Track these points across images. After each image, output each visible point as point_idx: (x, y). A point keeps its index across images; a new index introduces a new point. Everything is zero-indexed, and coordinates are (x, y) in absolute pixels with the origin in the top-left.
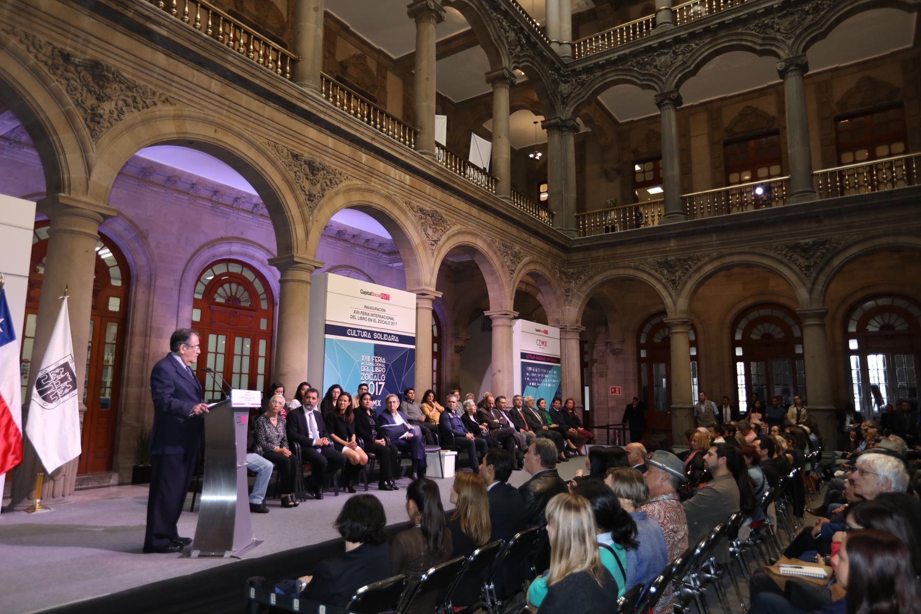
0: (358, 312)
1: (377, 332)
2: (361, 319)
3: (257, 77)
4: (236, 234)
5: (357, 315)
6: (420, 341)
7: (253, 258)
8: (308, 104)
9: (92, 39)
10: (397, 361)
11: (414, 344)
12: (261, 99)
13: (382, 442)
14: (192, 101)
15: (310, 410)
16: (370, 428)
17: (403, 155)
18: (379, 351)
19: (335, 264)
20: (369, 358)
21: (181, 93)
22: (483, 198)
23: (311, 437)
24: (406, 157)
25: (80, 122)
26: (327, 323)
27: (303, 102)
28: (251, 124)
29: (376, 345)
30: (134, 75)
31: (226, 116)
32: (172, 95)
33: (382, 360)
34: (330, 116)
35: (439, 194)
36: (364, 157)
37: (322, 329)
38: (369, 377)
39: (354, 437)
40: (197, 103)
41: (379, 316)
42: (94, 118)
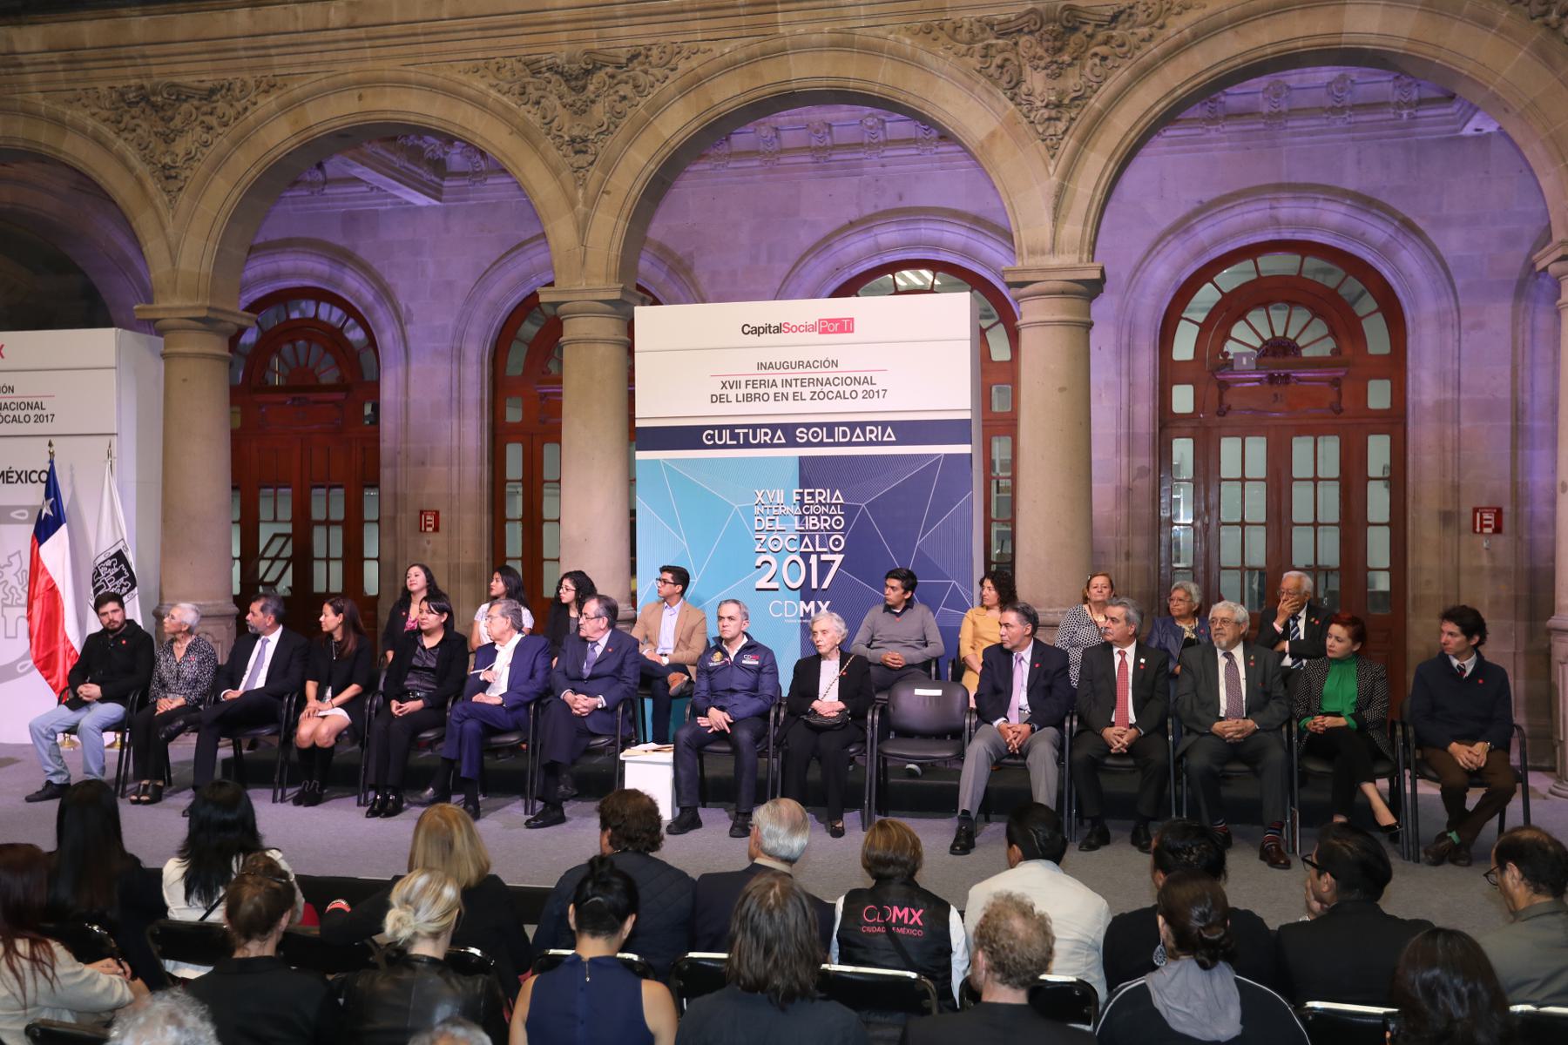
1: (808, 426)
2: (748, 398)
4: (887, 203)
5: (732, 393)
7: (936, 246)
9: (148, 50)
14: (309, 64)
18: (811, 474)
19: (1207, 197)
20: (784, 493)
21: (288, 59)
25: (152, 185)
29: (801, 459)
30: (215, 71)
31: (373, 59)
32: (277, 72)
40: (318, 63)
41: (811, 382)
42: (168, 174)
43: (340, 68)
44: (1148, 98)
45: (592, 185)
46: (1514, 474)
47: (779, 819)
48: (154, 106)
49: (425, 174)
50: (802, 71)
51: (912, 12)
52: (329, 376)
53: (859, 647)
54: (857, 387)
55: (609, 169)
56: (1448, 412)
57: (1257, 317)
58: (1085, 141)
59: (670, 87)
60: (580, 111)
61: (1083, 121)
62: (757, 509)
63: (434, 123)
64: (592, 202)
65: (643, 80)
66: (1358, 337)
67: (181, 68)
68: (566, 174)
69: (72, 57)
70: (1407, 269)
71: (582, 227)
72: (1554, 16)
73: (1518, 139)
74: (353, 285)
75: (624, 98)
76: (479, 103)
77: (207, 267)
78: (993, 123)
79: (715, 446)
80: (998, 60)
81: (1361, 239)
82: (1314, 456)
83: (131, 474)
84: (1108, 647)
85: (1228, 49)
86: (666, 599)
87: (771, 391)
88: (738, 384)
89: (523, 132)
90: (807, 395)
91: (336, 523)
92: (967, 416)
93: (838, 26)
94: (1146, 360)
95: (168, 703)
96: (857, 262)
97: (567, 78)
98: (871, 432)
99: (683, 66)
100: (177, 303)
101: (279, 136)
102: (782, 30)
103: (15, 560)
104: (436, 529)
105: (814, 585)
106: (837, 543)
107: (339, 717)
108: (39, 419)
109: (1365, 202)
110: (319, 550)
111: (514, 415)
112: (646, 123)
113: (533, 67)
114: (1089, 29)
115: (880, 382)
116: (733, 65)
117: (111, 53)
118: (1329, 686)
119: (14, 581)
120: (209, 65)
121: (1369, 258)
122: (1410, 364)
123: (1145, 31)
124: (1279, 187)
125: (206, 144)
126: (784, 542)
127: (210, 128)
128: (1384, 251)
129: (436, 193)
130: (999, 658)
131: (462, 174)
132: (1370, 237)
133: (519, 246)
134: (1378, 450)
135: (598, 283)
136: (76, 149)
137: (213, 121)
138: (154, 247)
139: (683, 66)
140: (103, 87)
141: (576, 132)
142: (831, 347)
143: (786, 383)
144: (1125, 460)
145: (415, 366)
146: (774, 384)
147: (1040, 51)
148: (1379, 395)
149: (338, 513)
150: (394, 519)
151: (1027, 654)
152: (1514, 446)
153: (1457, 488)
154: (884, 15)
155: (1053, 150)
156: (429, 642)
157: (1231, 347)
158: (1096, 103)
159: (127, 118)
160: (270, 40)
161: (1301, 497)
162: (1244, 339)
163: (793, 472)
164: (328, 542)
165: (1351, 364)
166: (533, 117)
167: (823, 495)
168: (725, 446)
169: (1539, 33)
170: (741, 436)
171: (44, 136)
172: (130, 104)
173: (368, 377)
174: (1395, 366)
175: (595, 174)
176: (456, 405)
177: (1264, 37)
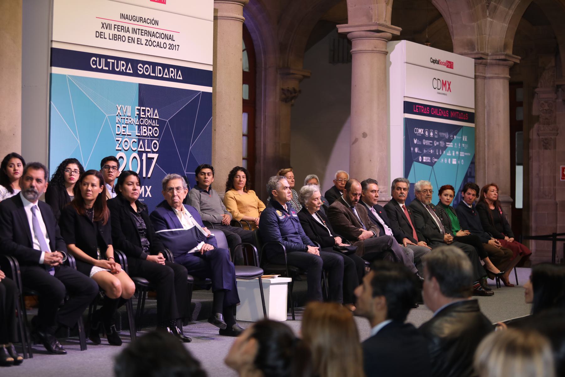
0: (108, 26)
1: (144, 63)
2: (116, 38)
5: (107, 32)
6: (220, 79)
10: (178, 116)
11: (210, 85)
13: (159, 258)
15: (32, 201)
16: (137, 233)
18: (147, 96)
20: (131, 109)
23: (36, 247)
26: (55, 45)
29: (140, 85)
33: (153, 113)
37: (46, 57)
38: (130, 144)
39: (110, 251)
54: (165, 41)
62: (117, 118)
79: (97, 70)
87: (127, 35)
90: (144, 42)
98: (172, 72)
105: (144, 175)
143: (134, 31)
163: (135, 95)
168: (102, 71)
170: (111, 64)
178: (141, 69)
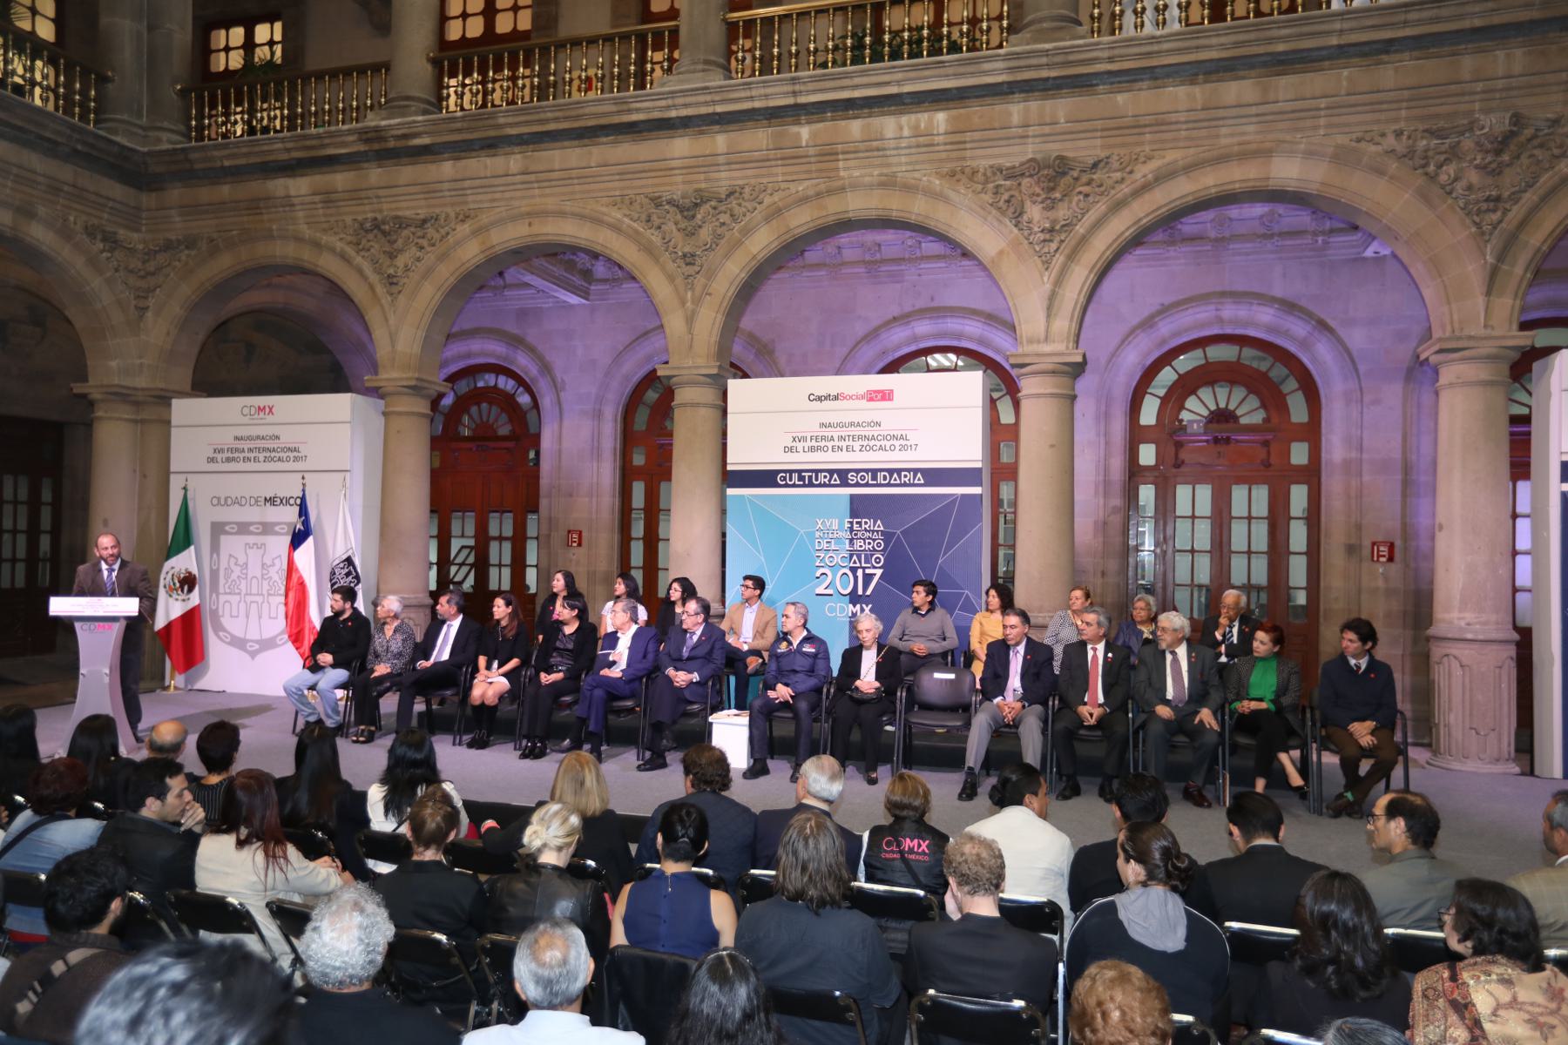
1: (857, 471)
2: (812, 449)
3: (547, 121)
4: (921, 303)
5: (800, 446)
7: (959, 336)
8: (638, 110)
9: (381, 193)
12: (586, 141)
14: (494, 200)
17: (887, 83)
18: (859, 507)
19: (1168, 300)
20: (838, 523)
21: (480, 197)
22: (1237, 44)
24: (899, 83)
25: (380, 290)
27: (629, 111)
28: (577, 188)
29: (852, 497)
30: (429, 206)
32: (472, 206)
34: (686, 106)
35: (1062, 108)
36: (805, 132)
42: (391, 281)
43: (516, 203)
44: (1120, 226)
45: (698, 289)
46: (1404, 515)
47: (821, 769)
48: (384, 233)
49: (577, 280)
50: (857, 204)
51: (941, 160)
52: (504, 430)
53: (893, 639)
55: (711, 276)
56: (1352, 468)
57: (1205, 393)
58: (1072, 257)
59: (757, 216)
60: (691, 234)
61: (1071, 241)
63: (583, 244)
64: (697, 301)
65: (738, 210)
66: (1284, 409)
67: (403, 204)
68: (679, 280)
69: (328, 198)
70: (1321, 358)
71: (690, 320)
72: (1432, 168)
73: (1406, 260)
74: (523, 363)
75: (723, 224)
76: (616, 228)
77: (417, 349)
78: (1002, 244)
79: (787, 486)
80: (1006, 197)
81: (1286, 334)
82: (1249, 500)
83: (359, 499)
84: (1082, 645)
85: (1182, 189)
86: (748, 601)
87: (830, 444)
88: (805, 439)
89: (648, 249)
90: (857, 448)
91: (507, 539)
92: (979, 465)
93: (885, 171)
94: (1119, 426)
95: (381, 669)
96: (899, 347)
97: (681, 209)
99: (768, 200)
100: (395, 375)
101: (471, 253)
102: (842, 173)
103: (277, 561)
104: (580, 545)
106: (878, 560)
107: (502, 683)
108: (296, 459)
109: (1289, 307)
110: (494, 559)
111: (639, 460)
112: (739, 243)
113: (656, 201)
114: (1075, 174)
115: (913, 438)
116: (804, 200)
117: (355, 195)
118: (1255, 678)
119: (276, 577)
120: (423, 203)
121: (1293, 349)
122: (1324, 431)
123: (1118, 175)
124: (1223, 294)
125: (418, 260)
126: (837, 559)
127: (422, 248)
128: (1304, 344)
129: (585, 294)
130: (999, 650)
131: (605, 281)
132: (1293, 333)
133: (646, 333)
134: (1299, 496)
135: (701, 361)
136: (329, 265)
137: (424, 242)
138: (380, 334)
139: (768, 200)
140: (348, 219)
141: (687, 249)
142: (877, 411)
143: (842, 438)
144: (1102, 501)
145: (566, 423)
146: (832, 439)
147: (1038, 190)
148: (1299, 454)
149: (508, 531)
150: (549, 536)
151: (1021, 649)
152: (1404, 495)
153: (1359, 527)
154: (917, 162)
155: (1047, 264)
156: (569, 630)
157: (1185, 416)
158: (1080, 229)
159: (364, 242)
160: (467, 184)
161: (1238, 533)
162: (1196, 409)
163: (845, 507)
164: (500, 553)
165: (1277, 431)
166: (656, 238)
167: (868, 523)
168: (794, 486)
169: (1420, 181)
170: (807, 478)
171: (306, 256)
172: (367, 231)
173: (532, 430)
174: (1312, 432)
175: (700, 281)
176: (596, 452)
177: (1209, 181)
178: (852, 478)
